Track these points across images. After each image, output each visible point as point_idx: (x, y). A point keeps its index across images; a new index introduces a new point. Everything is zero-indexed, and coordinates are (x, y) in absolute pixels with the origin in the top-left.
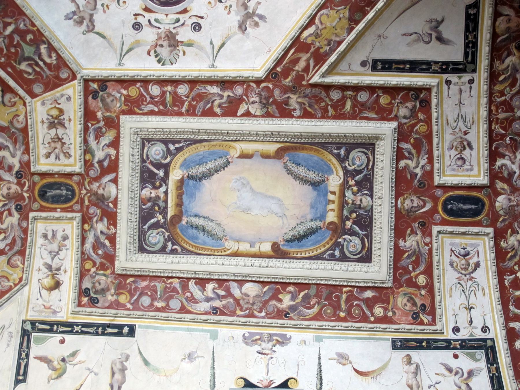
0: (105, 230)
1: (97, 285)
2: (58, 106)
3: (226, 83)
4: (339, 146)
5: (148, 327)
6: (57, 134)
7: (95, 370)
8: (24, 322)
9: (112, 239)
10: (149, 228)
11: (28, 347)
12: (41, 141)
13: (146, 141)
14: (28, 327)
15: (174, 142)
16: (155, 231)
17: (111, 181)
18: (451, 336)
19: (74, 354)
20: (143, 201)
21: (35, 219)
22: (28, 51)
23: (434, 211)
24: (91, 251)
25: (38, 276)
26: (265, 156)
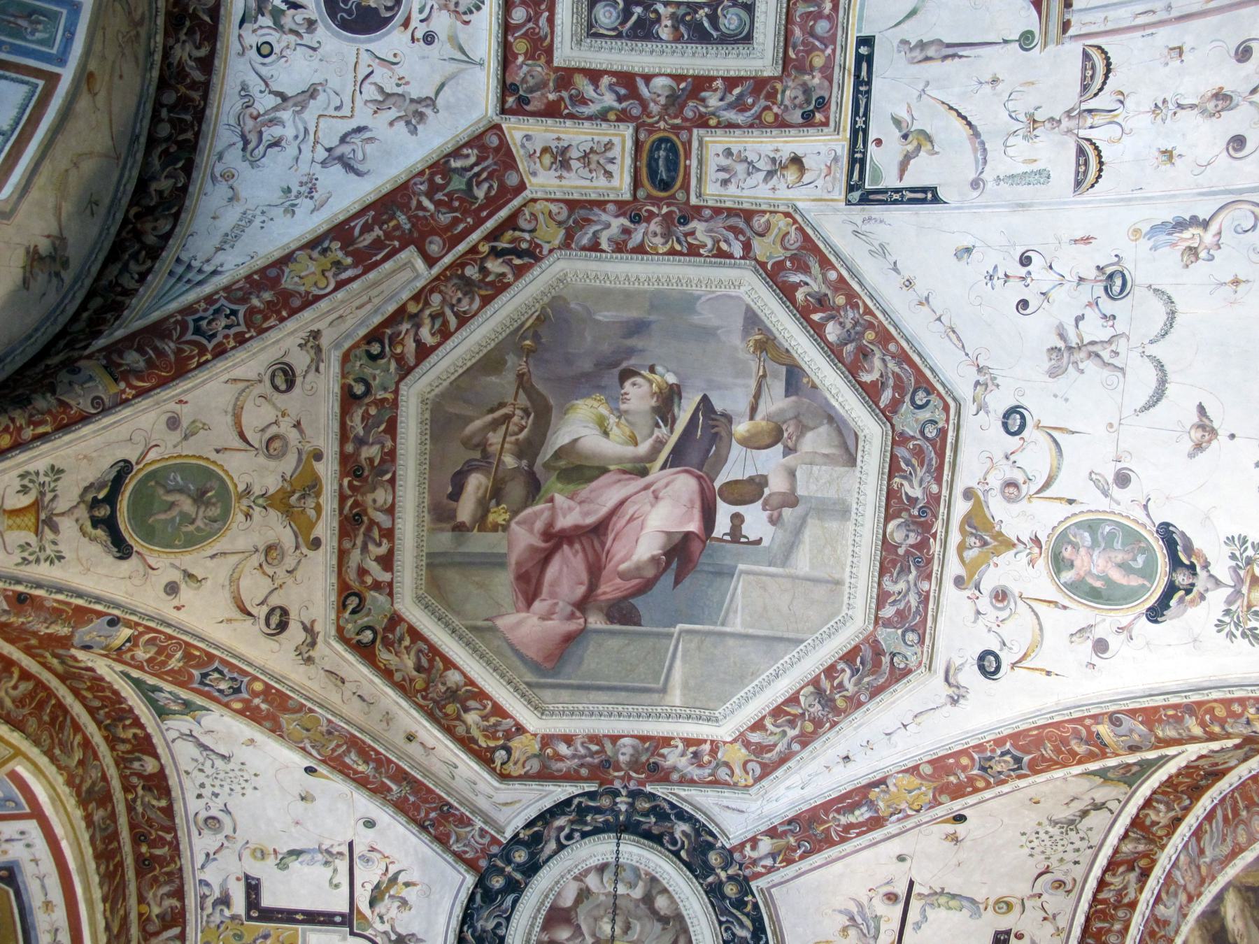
0: (719, 94)
1: (797, 101)
2: (538, 154)
5: (861, 18)
6: (578, 159)
7: (921, 87)
8: (848, 203)
9: (731, 82)
10: (717, 28)
11: (884, 191)
12: (587, 183)
13: (591, 31)
14: (856, 195)
16: (722, 20)
17: (647, 85)
19: (897, 122)
20: (678, 39)
21: (699, 196)
22: (458, 184)
24: (748, 114)
25: (784, 191)
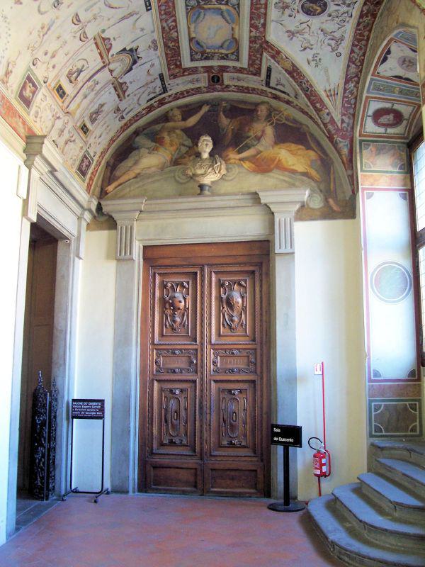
3: (264, 25)
4: (238, 53)
15: (239, 7)
18: (166, 84)
23: (213, 73)
26: (233, 34)
